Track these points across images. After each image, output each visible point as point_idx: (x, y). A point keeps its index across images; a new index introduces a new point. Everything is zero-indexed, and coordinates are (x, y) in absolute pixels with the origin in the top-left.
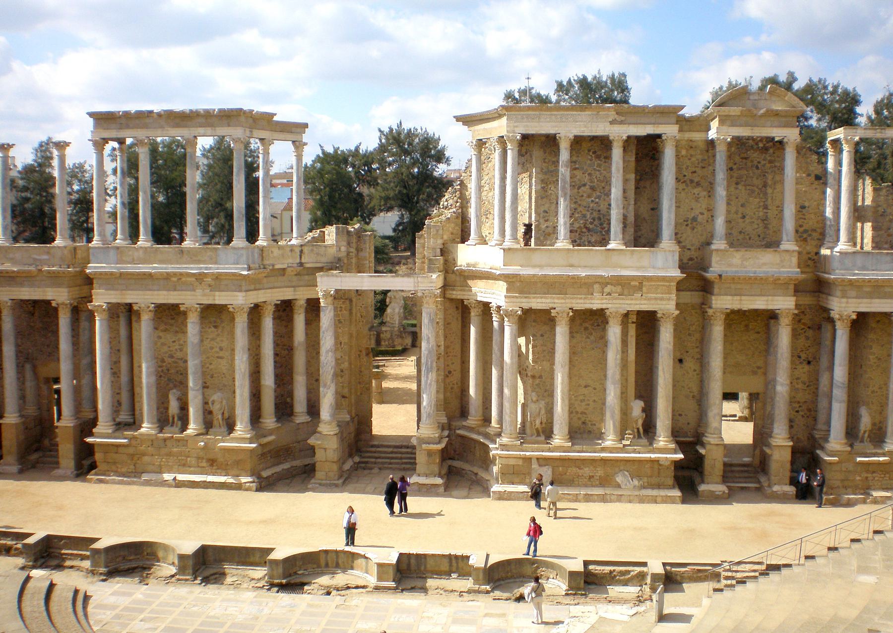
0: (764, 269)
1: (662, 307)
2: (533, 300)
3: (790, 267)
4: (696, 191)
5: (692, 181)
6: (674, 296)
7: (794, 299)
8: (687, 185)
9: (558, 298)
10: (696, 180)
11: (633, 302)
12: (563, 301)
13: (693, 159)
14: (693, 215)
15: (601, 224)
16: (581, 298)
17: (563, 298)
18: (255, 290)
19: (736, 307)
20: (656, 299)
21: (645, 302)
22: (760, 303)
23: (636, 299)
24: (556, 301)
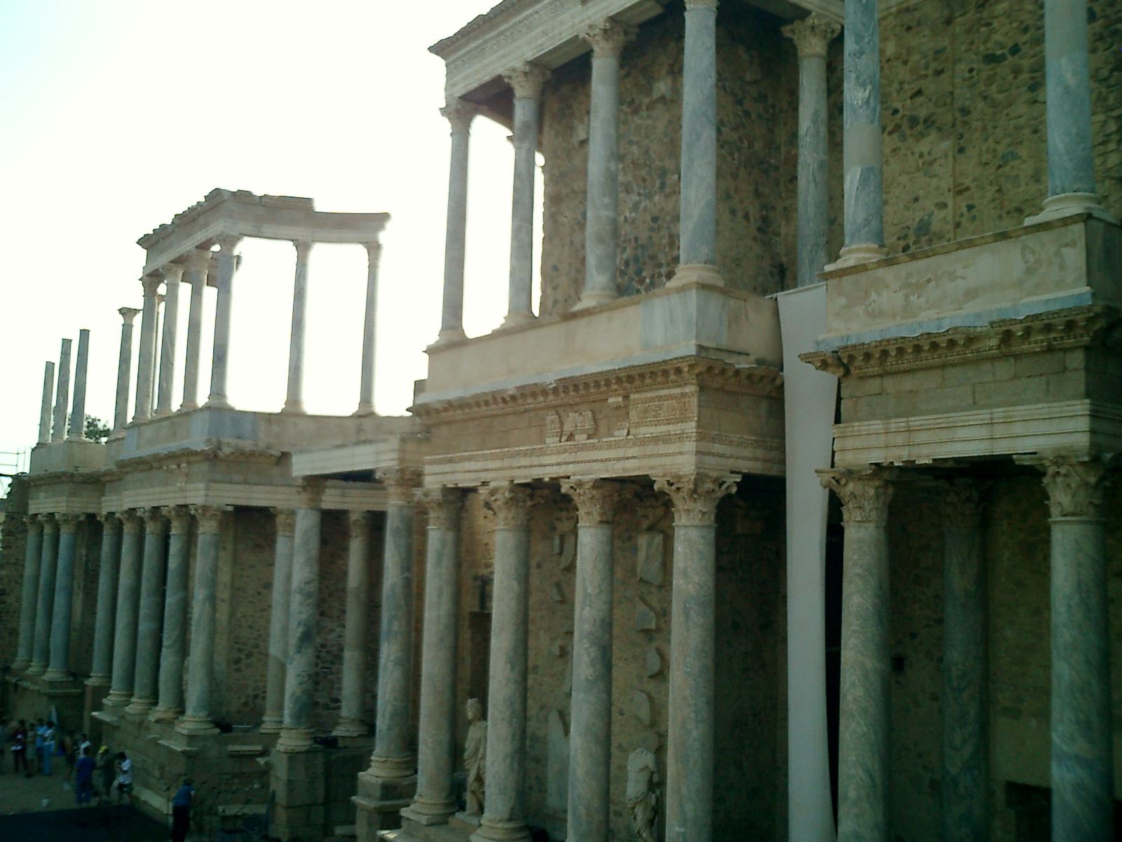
0: (973, 307)
1: (667, 461)
2: (459, 467)
3: (1060, 285)
4: (924, 146)
5: (913, 121)
6: (691, 427)
7: (1088, 401)
8: (904, 138)
9: (494, 457)
10: (922, 113)
11: (612, 454)
12: (498, 464)
13: (915, 58)
14: (919, 215)
15: (639, 272)
16: (525, 454)
17: (501, 457)
18: (246, 482)
19: (898, 456)
20: (655, 440)
21: (634, 451)
22: (966, 437)
23: (617, 445)
24: (490, 465)
